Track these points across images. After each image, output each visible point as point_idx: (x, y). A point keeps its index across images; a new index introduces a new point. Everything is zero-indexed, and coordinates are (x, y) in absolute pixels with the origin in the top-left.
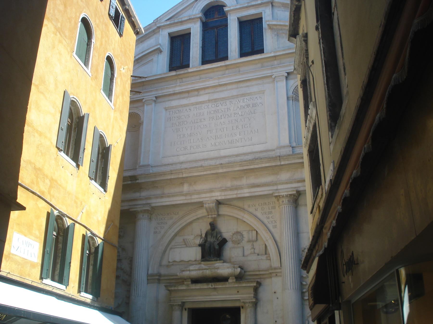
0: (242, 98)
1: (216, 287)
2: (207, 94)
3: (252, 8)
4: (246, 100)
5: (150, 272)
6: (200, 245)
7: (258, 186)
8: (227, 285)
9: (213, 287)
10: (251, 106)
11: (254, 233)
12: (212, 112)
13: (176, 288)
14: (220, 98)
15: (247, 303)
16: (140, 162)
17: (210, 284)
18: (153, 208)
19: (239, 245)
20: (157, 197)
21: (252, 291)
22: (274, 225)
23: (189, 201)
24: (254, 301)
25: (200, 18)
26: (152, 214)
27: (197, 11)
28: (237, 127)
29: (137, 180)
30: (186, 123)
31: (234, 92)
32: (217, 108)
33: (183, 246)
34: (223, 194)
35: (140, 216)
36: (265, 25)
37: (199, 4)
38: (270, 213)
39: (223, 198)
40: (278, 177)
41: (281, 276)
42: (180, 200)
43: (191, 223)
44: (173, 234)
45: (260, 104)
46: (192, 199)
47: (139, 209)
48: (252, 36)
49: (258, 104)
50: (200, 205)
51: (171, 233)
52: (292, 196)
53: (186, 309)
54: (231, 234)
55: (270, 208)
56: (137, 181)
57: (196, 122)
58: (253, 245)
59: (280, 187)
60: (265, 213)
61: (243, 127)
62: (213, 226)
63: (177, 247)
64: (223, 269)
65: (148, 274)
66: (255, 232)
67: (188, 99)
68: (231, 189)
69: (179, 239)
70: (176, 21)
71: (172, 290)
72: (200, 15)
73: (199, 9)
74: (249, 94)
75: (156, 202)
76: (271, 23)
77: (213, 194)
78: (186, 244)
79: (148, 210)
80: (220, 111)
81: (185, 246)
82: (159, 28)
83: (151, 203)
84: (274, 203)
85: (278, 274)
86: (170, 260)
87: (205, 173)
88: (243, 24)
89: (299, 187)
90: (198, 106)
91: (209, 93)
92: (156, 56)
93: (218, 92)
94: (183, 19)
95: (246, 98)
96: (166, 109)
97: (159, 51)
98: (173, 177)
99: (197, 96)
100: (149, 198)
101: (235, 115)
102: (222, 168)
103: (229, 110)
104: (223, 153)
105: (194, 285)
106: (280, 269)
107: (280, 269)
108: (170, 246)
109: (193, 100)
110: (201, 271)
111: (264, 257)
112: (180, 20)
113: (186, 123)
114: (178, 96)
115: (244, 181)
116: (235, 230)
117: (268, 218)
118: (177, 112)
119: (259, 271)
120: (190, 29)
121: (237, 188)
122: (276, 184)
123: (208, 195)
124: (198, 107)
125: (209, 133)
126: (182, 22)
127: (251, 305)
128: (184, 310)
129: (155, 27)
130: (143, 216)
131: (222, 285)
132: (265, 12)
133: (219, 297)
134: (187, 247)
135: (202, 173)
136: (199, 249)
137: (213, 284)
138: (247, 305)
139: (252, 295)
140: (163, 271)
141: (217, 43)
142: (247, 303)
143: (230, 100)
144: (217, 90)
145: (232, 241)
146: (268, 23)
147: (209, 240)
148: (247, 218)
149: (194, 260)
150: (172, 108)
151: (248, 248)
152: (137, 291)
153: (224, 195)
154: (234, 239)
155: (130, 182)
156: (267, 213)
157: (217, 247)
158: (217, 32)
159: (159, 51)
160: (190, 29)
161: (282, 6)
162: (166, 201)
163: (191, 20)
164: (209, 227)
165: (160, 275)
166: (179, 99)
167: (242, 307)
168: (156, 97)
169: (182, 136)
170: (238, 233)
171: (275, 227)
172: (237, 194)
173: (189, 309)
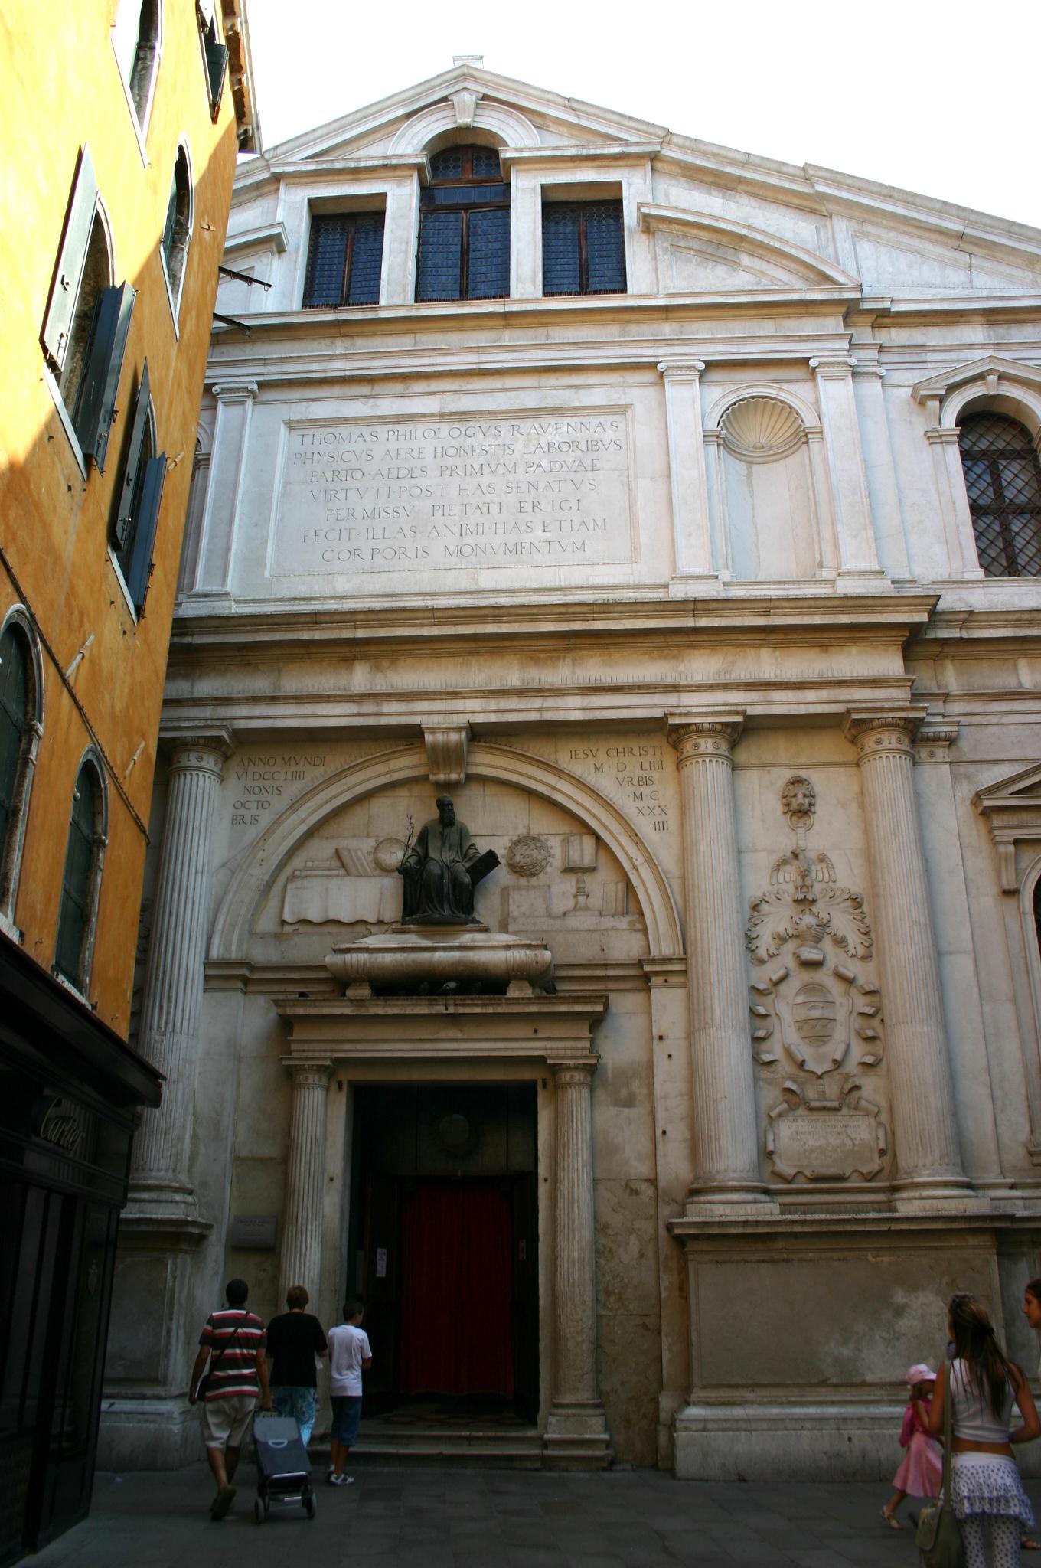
0: (553, 421)
1: (461, 1010)
2: (435, 393)
3: (589, 164)
4: (565, 428)
5: (215, 953)
6: (403, 870)
9: (451, 1010)
10: (583, 446)
11: (588, 843)
12: (451, 452)
14: (481, 413)
16: (192, 585)
19: (534, 881)
22: (657, 819)
23: (371, 721)
25: (419, 168)
27: (412, 143)
28: (535, 506)
30: (358, 475)
31: (531, 400)
32: (469, 441)
33: (335, 872)
34: (493, 704)
36: (630, 216)
37: (416, 129)
38: (647, 781)
39: (493, 718)
40: (681, 668)
44: (304, 828)
45: (613, 447)
48: (580, 248)
49: (606, 443)
50: (410, 736)
52: (729, 731)
53: (340, 1084)
55: (646, 766)
57: (394, 474)
59: (688, 699)
60: (630, 781)
61: (556, 508)
63: (314, 873)
65: (207, 957)
67: (371, 402)
68: (521, 693)
69: (321, 850)
70: (338, 165)
72: (421, 160)
73: (415, 142)
74: (575, 410)
76: (654, 212)
77: (459, 704)
79: (219, 740)
80: (478, 450)
81: (342, 872)
82: (277, 178)
83: (234, 719)
86: (287, 917)
88: (558, 209)
90: (401, 428)
91: (443, 393)
92: (265, 260)
93: (473, 392)
94: (362, 164)
95: (566, 420)
96: (291, 425)
97: (274, 243)
99: (402, 396)
101: (531, 470)
103: (508, 451)
104: (487, 580)
107: (683, 960)
108: (288, 871)
109: (387, 406)
111: (623, 923)
112: (352, 165)
113: (358, 475)
114: (337, 391)
117: (640, 797)
118: (330, 438)
119: (606, 966)
120: (383, 196)
122: (675, 688)
123: (439, 705)
124: (402, 432)
125: (439, 513)
126: (357, 173)
128: (334, 1086)
129: (265, 175)
130: (200, 759)
131: (483, 1005)
132: (629, 184)
134: (348, 874)
136: (392, 885)
138: (566, 1077)
141: (465, 252)
143: (513, 422)
144: (470, 387)
146: (644, 210)
147: (432, 854)
149: (373, 920)
150: (314, 423)
152: (168, 1013)
154: (518, 858)
156: (636, 782)
157: (467, 880)
158: (468, 220)
159: (274, 243)
160: (383, 196)
161: (684, 176)
163: (388, 169)
164: (435, 813)
166: (338, 398)
168: (260, 384)
169: (344, 514)
172: (540, 710)
173: (350, 1082)
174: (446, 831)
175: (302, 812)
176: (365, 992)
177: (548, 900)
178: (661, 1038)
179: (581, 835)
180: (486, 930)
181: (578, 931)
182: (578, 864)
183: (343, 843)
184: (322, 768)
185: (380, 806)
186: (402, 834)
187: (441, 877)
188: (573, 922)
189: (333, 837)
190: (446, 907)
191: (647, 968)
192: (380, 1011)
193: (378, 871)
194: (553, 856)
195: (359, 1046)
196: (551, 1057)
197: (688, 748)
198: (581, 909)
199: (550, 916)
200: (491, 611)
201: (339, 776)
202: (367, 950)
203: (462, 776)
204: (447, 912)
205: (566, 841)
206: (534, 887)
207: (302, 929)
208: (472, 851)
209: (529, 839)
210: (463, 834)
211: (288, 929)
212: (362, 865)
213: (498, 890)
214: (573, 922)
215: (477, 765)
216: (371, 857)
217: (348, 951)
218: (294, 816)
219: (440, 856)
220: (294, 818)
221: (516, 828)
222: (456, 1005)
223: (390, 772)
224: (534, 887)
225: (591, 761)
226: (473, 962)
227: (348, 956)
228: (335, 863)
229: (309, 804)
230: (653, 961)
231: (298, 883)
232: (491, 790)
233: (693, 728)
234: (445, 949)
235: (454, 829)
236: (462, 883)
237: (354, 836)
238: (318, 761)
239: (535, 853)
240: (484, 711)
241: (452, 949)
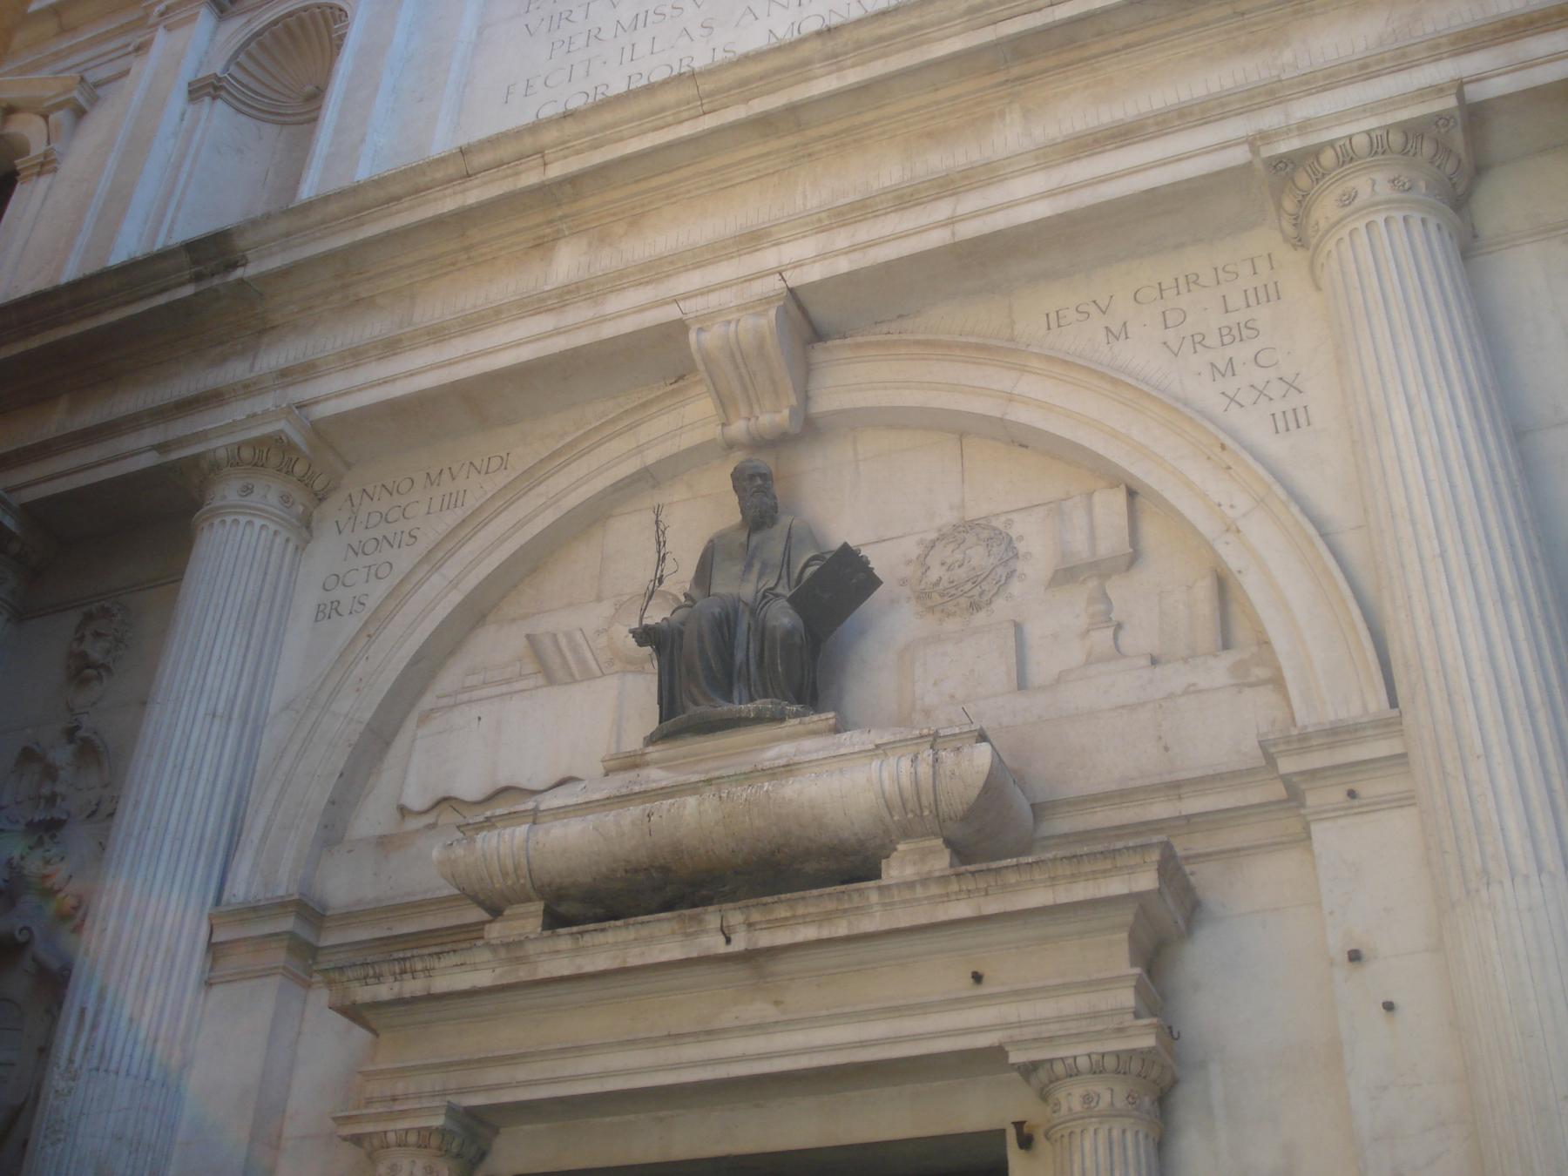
1: (765, 939)
7: (1123, 135)
8: (871, 911)
9: (739, 944)
11: (1111, 505)
13: (413, 986)
15: (1073, 1073)
17: (712, 917)
18: (322, 432)
19: (980, 618)
20: (355, 356)
21: (1113, 957)
24: (1148, 1041)
26: (320, 498)
29: (234, 266)
34: (841, 239)
35: (227, 492)
39: (843, 266)
41: (1406, 800)
42: (518, 344)
43: (592, 517)
46: (603, 319)
47: (219, 445)
51: (438, 597)
52: (1428, 148)
54: (911, 547)
55: (1236, 300)
56: (239, 273)
58: (1106, 599)
59: (1305, 109)
60: (1198, 341)
62: (760, 497)
64: (825, 775)
65: (218, 900)
66: (1120, 497)
68: (905, 199)
69: (498, 645)
71: (376, 1005)
75: (345, 391)
77: (769, 258)
78: (548, 666)
79: (279, 443)
83: (316, 402)
84: (1263, 266)
85: (1370, 788)
87: (708, 122)
89: (1478, 79)
98: (474, 195)
100: (307, 370)
102: (834, 60)
105: (564, 939)
106: (1390, 724)
110: (635, 811)
111: (1218, 671)
115: (1010, 135)
116: (947, 518)
119: (1175, 788)
121: (948, 186)
127: (1109, 1093)
130: (247, 490)
131: (827, 918)
133: (798, 1039)
135: (685, 130)
137: (735, 918)
138: (1071, 1097)
139: (1126, 997)
140: (343, 885)
142: (1073, 1073)
145: (922, 596)
148: (1041, 401)
151: (1057, 626)
152: (94, 1027)
153: (852, 249)
154: (935, 573)
155: (188, 291)
156: (1213, 340)
162: (421, 370)
165: (310, 911)
167: (1026, 1142)
169: (580, 41)
170: (964, 529)
171: (1293, 421)
172: (951, 221)
176: (527, 921)
178: (1355, 956)
191: (1287, 765)
192: (562, 967)
194: (1028, 555)
195: (522, 1073)
196: (1020, 1043)
197: (1326, 209)
200: (816, 45)
211: (413, 824)
218: (436, 578)
222: (750, 925)
230: (1303, 741)
233: (1328, 158)
240: (821, 257)
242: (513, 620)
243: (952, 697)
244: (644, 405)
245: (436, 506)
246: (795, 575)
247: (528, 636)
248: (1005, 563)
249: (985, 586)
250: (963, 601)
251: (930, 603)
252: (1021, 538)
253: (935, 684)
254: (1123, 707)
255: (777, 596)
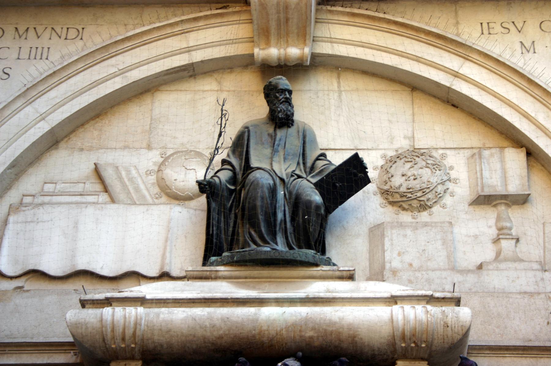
11: (515, 159)
19: (424, 216)
44: (44, 127)
63: (55, 199)
69: (70, 165)
81: (103, 197)
116: (403, 144)
154: (397, 181)
157: (317, 198)
164: (261, 109)
174: (281, 133)
175: (42, 104)
177: (449, 244)
179: (502, 148)
180: (351, 277)
181: (504, 294)
182: (500, 190)
183: (106, 158)
184: (80, 44)
185: (169, 104)
186: (206, 145)
187: (273, 191)
188: (495, 279)
189: (91, 149)
190: (280, 239)
193: (164, 199)
194: (455, 181)
198: (506, 260)
199: (453, 269)
201: (106, 52)
202: (142, 301)
203: (307, 50)
204: (281, 246)
205: (476, 155)
206: (426, 225)
207: (29, 284)
208: (320, 163)
209: (414, 155)
210: (306, 139)
212: (137, 190)
213: (364, 230)
214: (495, 279)
215: (332, 41)
216: (152, 179)
217: (108, 302)
218: (29, 109)
219: (271, 166)
220: (29, 113)
221: (392, 139)
223: (189, 50)
224: (426, 225)
225: (514, 38)
226: (332, 323)
227: (107, 311)
228: (94, 186)
229: (52, 94)
231: (29, 214)
232: (351, 82)
234: (279, 302)
235: (292, 131)
236: (309, 204)
237: (126, 147)
238: (72, 33)
239: (426, 173)
241: (292, 302)
242: (82, 150)
243: (411, 265)
244: (195, 19)
245: (24, 54)
246: (309, 164)
247: (95, 164)
248: (443, 183)
249: (430, 196)
250: (415, 204)
251: (391, 200)
252: (451, 168)
253: (399, 254)
254: (525, 293)
255: (299, 177)
